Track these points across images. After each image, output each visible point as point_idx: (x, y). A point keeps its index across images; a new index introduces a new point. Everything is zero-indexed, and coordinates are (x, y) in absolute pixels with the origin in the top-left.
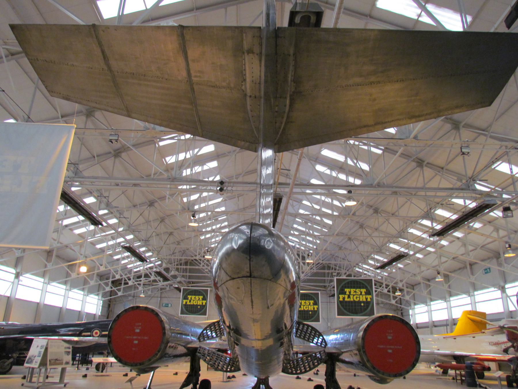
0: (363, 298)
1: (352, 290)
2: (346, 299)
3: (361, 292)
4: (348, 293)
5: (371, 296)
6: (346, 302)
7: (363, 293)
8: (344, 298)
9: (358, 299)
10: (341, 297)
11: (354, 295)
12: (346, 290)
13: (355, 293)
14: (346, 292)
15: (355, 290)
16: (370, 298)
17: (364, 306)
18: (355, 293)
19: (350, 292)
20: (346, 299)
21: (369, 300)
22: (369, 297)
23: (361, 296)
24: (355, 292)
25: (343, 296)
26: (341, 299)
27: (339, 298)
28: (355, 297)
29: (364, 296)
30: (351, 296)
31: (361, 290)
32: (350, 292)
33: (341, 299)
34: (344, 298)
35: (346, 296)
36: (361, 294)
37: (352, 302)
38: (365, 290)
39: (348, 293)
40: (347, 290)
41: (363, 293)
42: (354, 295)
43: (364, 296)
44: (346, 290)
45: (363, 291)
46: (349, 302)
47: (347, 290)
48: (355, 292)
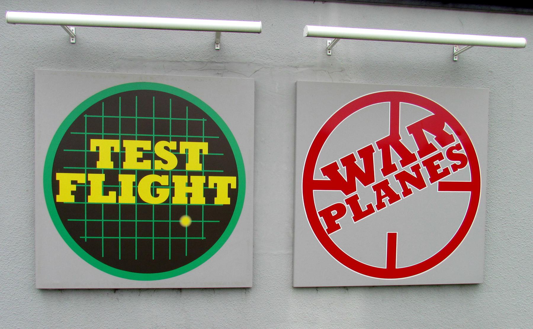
0: (189, 192)
1: (133, 148)
2: (96, 196)
3: (182, 160)
4: (105, 162)
5: (232, 180)
6: (95, 208)
7: (194, 164)
8: (82, 192)
9: (164, 194)
10: (66, 181)
11: (141, 174)
12: (94, 143)
13: (146, 165)
14: (95, 157)
15: (146, 145)
16: (233, 193)
17: (194, 229)
18: (146, 165)
19: (118, 158)
20: (96, 196)
21: (222, 199)
22: (222, 183)
23: (180, 181)
24: (149, 156)
25: (81, 178)
26: (66, 196)
27: (55, 187)
28: (147, 182)
29: (198, 181)
30: (126, 181)
31: (184, 146)
32: (118, 158)
33: (66, 196)
34: (82, 192)
35: (97, 181)
36: (181, 168)
37: (128, 208)
38: (204, 146)
39: (105, 162)
40: (104, 147)
41: (194, 164)
42: (141, 174)
43: (198, 181)
44: (94, 143)
45: (195, 150)
46: (111, 209)
47: (104, 147)
48: (149, 156)
